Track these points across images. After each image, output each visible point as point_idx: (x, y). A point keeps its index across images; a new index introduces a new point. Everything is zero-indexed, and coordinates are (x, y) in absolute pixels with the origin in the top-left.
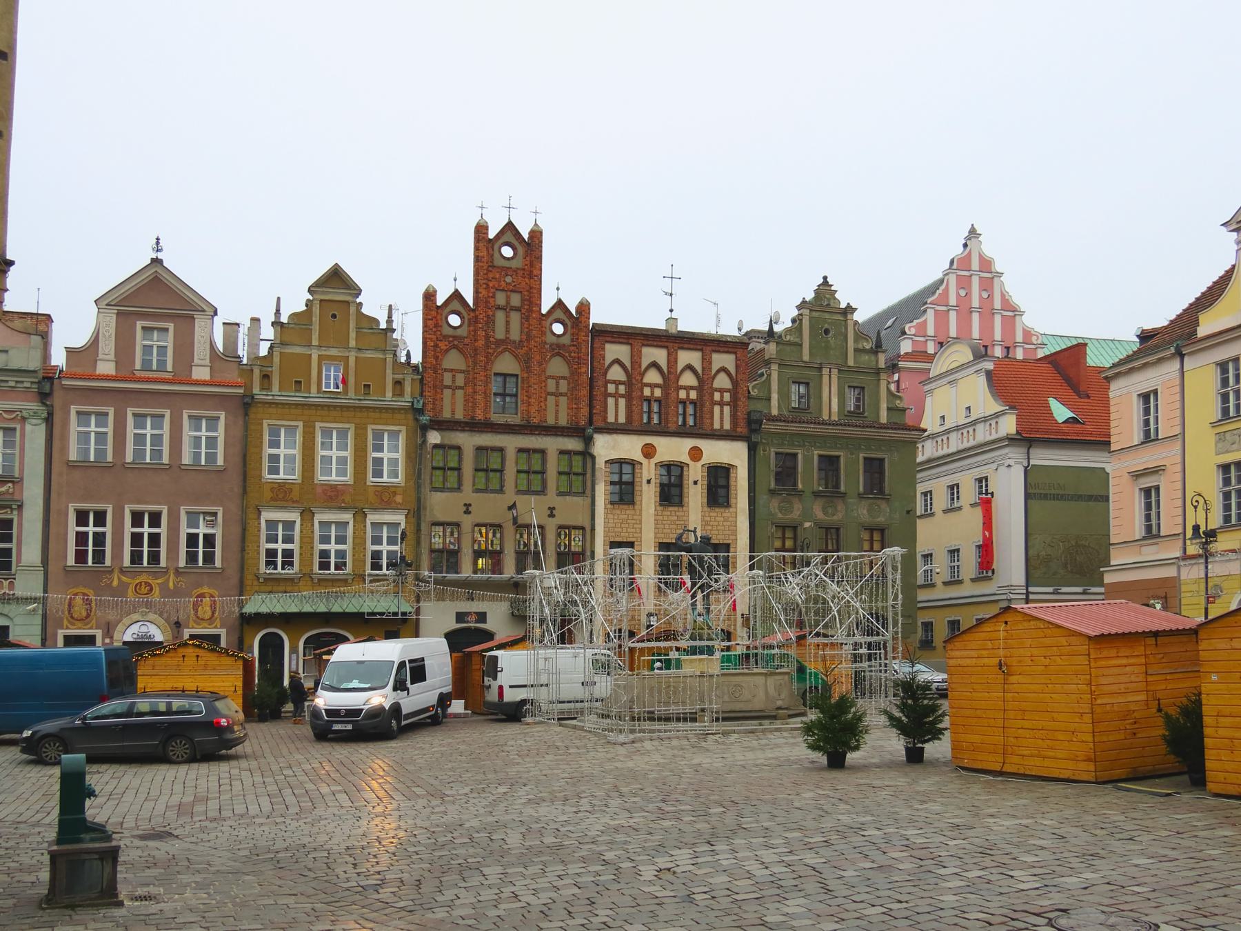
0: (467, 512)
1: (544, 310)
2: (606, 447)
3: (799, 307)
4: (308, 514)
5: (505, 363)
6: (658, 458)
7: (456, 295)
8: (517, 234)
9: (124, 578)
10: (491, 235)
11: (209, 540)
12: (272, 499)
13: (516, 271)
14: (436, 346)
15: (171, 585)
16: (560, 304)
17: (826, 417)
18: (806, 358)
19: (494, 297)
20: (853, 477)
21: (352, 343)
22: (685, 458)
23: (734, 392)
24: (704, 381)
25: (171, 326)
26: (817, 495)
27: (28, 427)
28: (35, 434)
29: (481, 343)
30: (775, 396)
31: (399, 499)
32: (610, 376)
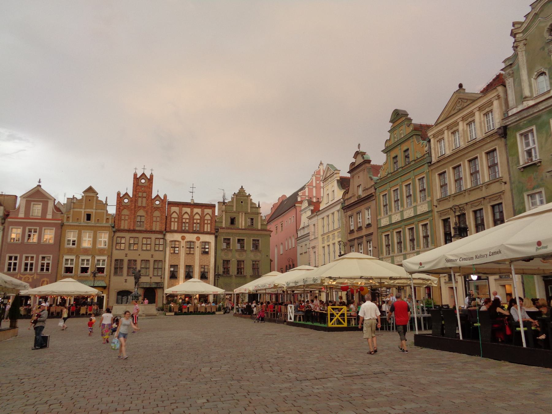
0: (126, 256)
1: (153, 198)
2: (170, 237)
3: (233, 195)
4: (78, 257)
6: (186, 240)
7: (126, 194)
8: (146, 176)
9: (21, 276)
10: (138, 177)
11: (48, 264)
13: (145, 187)
15: (35, 278)
16: (158, 196)
17: (240, 227)
18: (235, 210)
20: (249, 245)
22: (194, 240)
23: (211, 220)
24: (202, 218)
25: (41, 204)
26: (237, 251)
29: (133, 207)
30: (224, 222)
31: (106, 252)
32: (173, 216)
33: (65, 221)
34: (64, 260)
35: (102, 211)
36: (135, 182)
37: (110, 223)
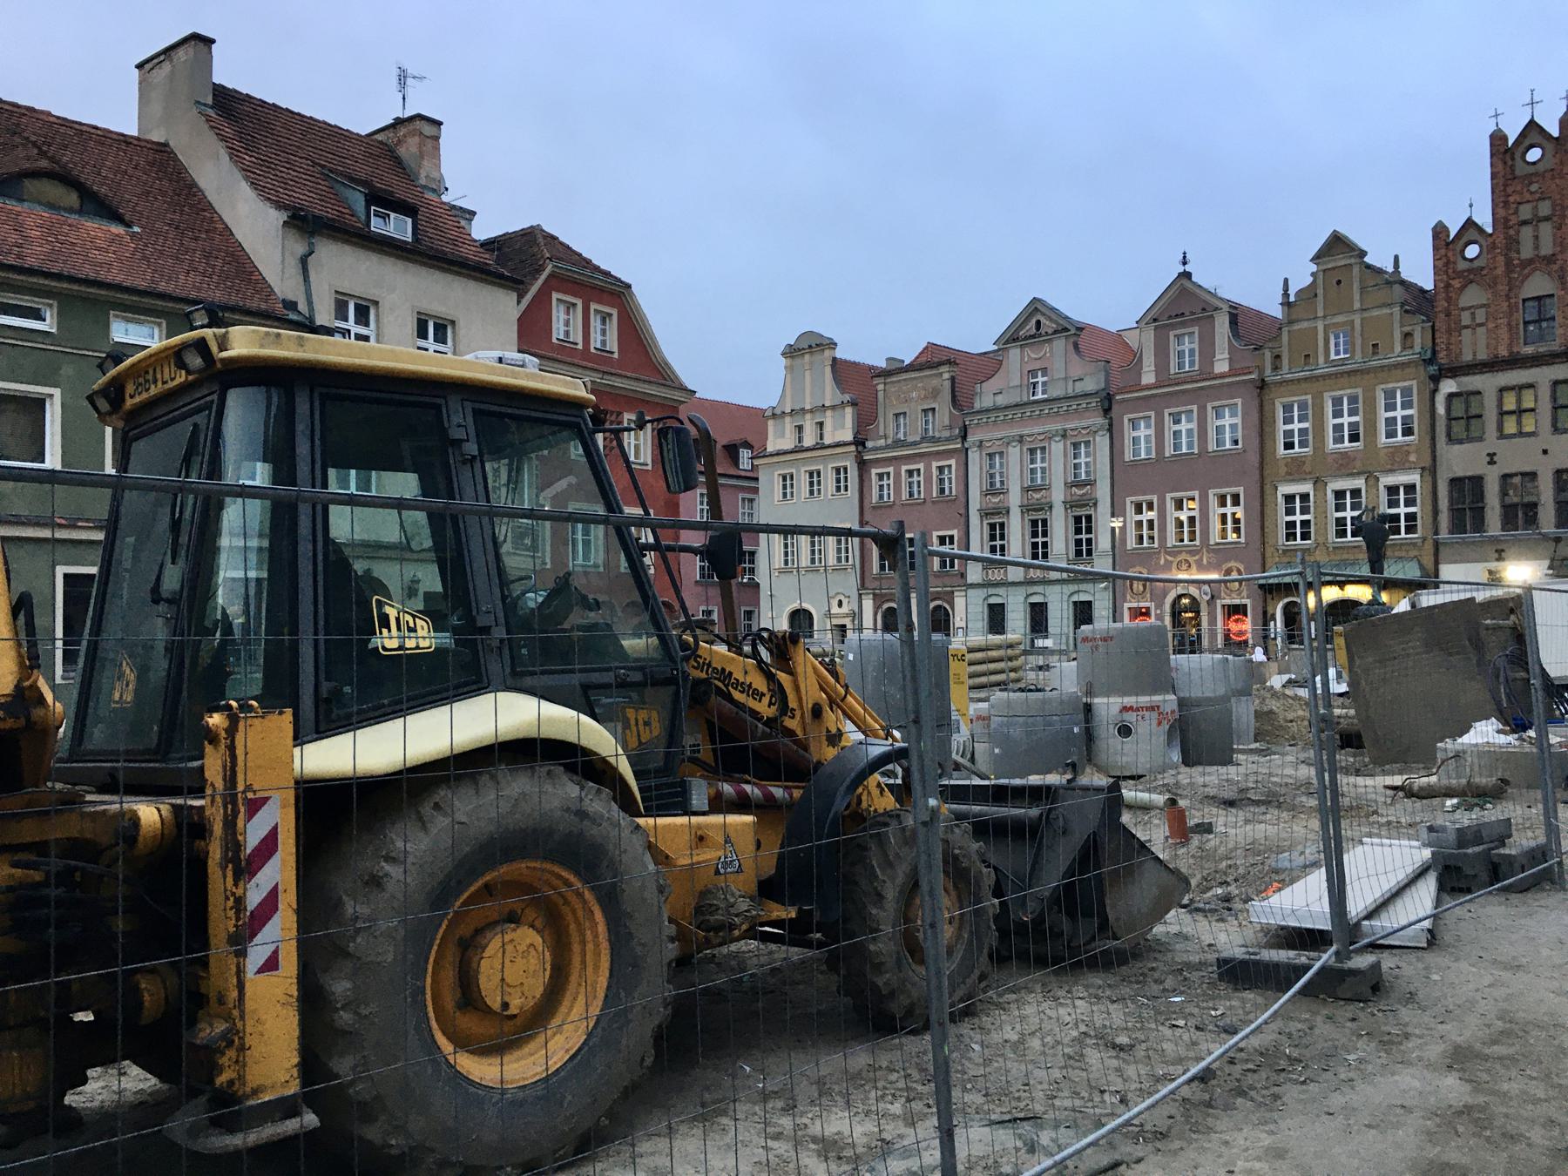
0: (1492, 463)
4: (1319, 483)
5: (1539, 284)
7: (1470, 224)
12: (1289, 474)
14: (1448, 286)
19: (1516, 212)
21: (1357, 305)
27: (1098, 439)
28: (1102, 442)
29: (1500, 271)
31: (1413, 458)
33: (1268, 372)
34: (1281, 500)
35: (1386, 311)
36: (1500, 166)
37: (1417, 349)
